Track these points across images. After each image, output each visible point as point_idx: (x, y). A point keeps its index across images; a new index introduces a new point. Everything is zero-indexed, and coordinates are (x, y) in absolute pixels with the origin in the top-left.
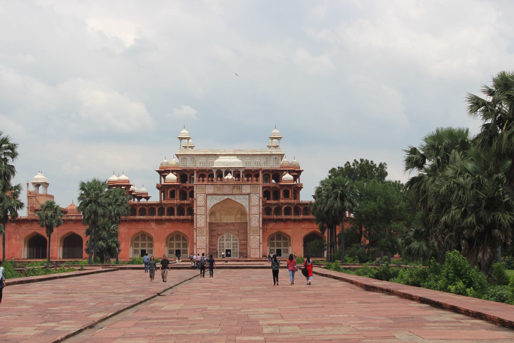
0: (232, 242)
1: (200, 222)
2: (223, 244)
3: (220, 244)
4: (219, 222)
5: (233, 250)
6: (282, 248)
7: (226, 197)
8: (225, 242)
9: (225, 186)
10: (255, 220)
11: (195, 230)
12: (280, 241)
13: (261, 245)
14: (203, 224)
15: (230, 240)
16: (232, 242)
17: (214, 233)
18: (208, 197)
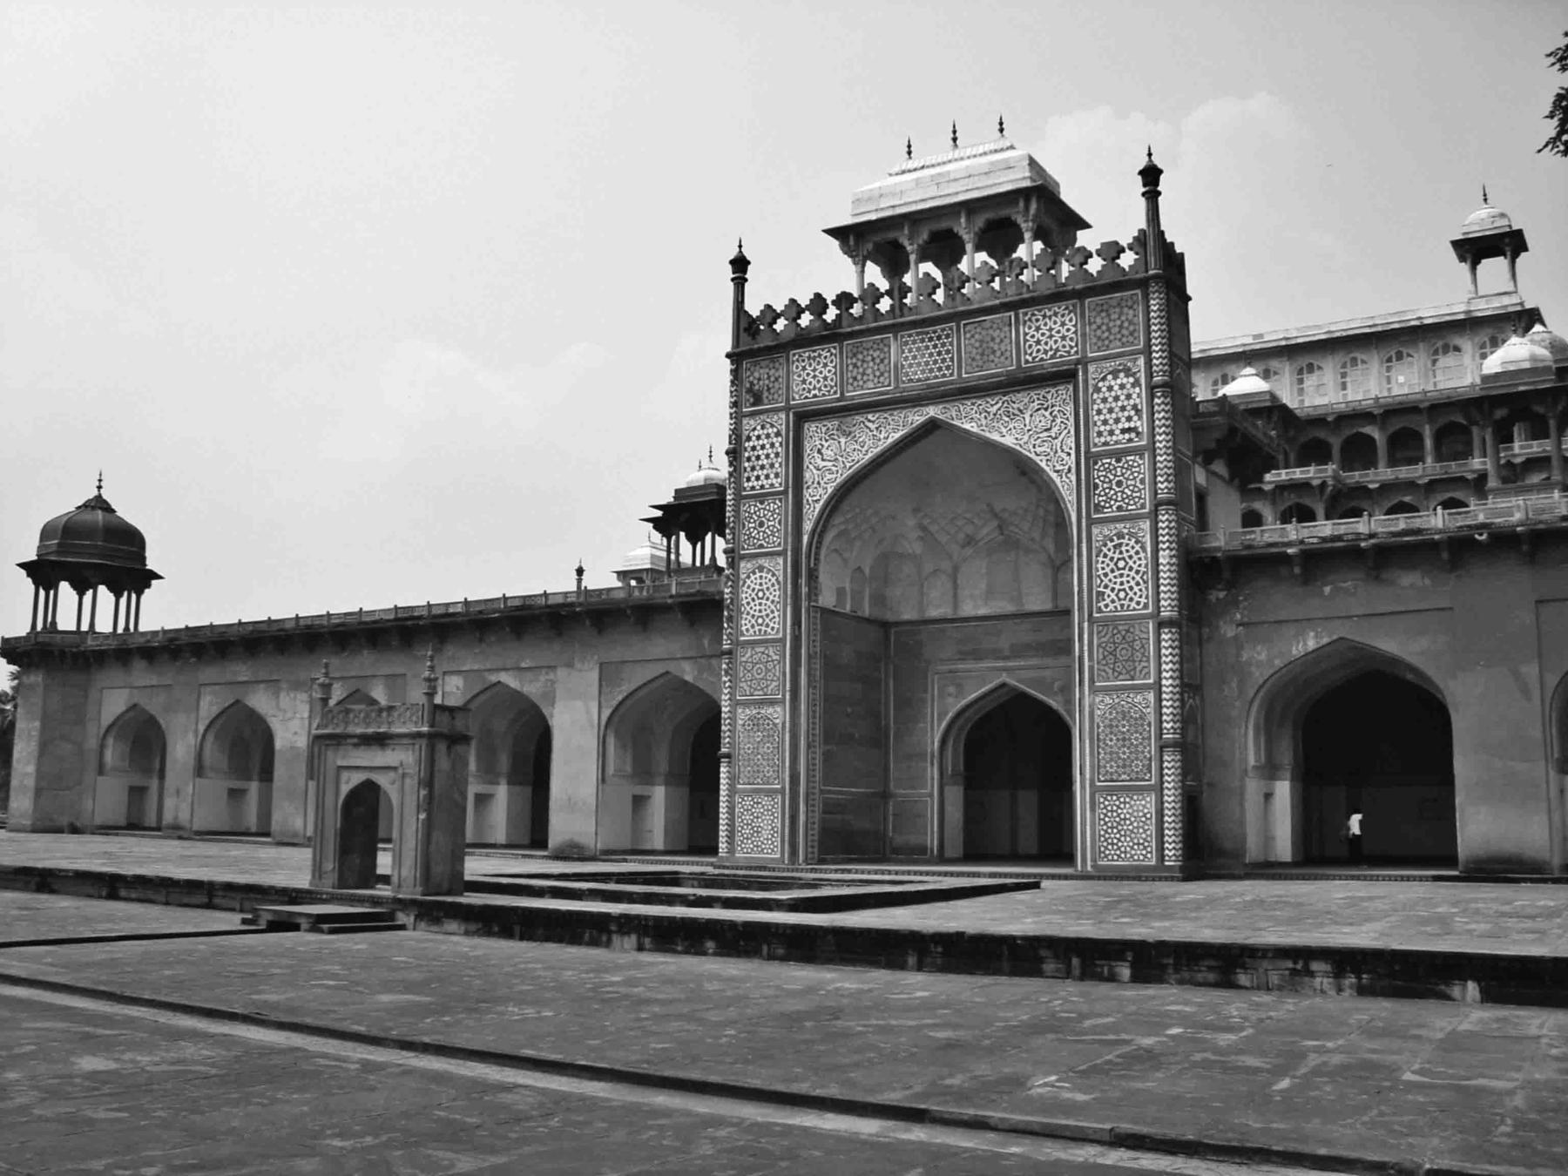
7: (917, 417)
18: (812, 429)
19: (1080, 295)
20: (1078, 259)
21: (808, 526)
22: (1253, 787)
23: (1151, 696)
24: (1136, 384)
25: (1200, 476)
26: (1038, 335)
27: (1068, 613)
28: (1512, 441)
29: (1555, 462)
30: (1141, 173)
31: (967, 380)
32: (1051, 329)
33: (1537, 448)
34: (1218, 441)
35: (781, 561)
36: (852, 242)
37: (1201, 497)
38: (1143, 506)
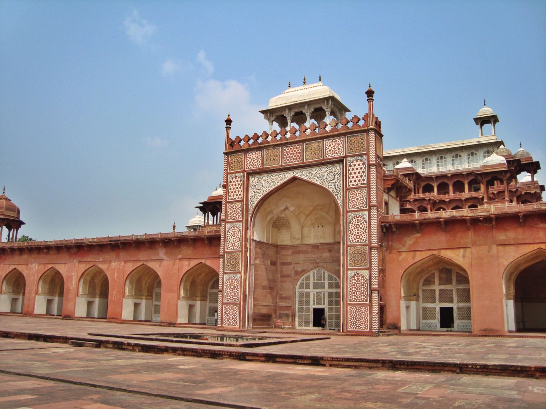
0: (327, 290)
1: (231, 240)
2: (308, 295)
3: (301, 295)
4: (298, 242)
5: (330, 310)
6: (454, 305)
7: (289, 175)
8: (312, 291)
9: (287, 149)
10: (357, 226)
11: (221, 260)
12: (448, 287)
13: (375, 295)
14: (238, 244)
15: (323, 287)
16: (327, 290)
17: (288, 270)
19: (344, 134)
20: (344, 121)
21: (250, 213)
22: (403, 304)
23: (367, 272)
24: (363, 164)
25: (386, 197)
26: (330, 148)
27: (339, 243)
28: (494, 185)
29: (506, 193)
30: (366, 93)
31: (305, 163)
32: (334, 146)
33: (501, 188)
34: (392, 185)
35: (241, 224)
36: (268, 115)
37: (386, 204)
38: (366, 207)
